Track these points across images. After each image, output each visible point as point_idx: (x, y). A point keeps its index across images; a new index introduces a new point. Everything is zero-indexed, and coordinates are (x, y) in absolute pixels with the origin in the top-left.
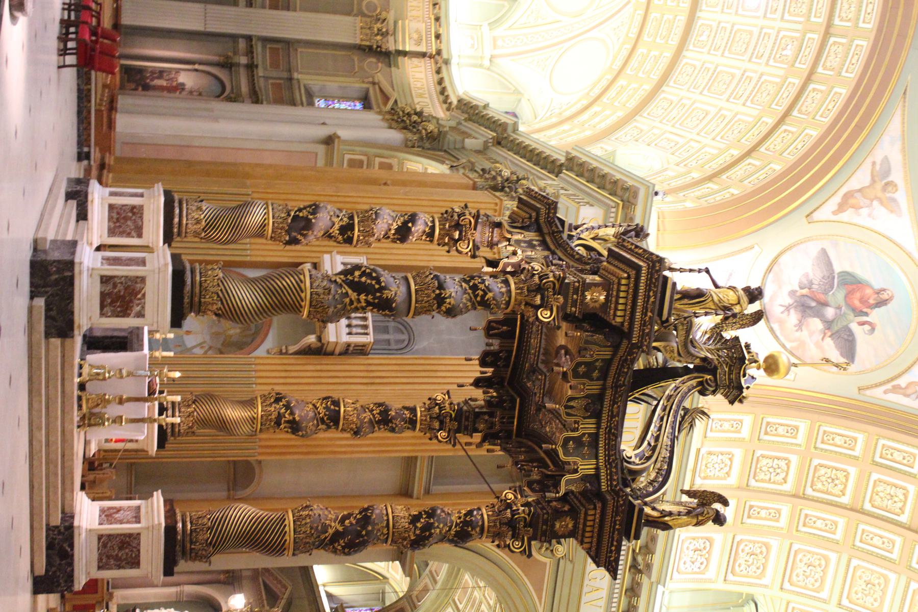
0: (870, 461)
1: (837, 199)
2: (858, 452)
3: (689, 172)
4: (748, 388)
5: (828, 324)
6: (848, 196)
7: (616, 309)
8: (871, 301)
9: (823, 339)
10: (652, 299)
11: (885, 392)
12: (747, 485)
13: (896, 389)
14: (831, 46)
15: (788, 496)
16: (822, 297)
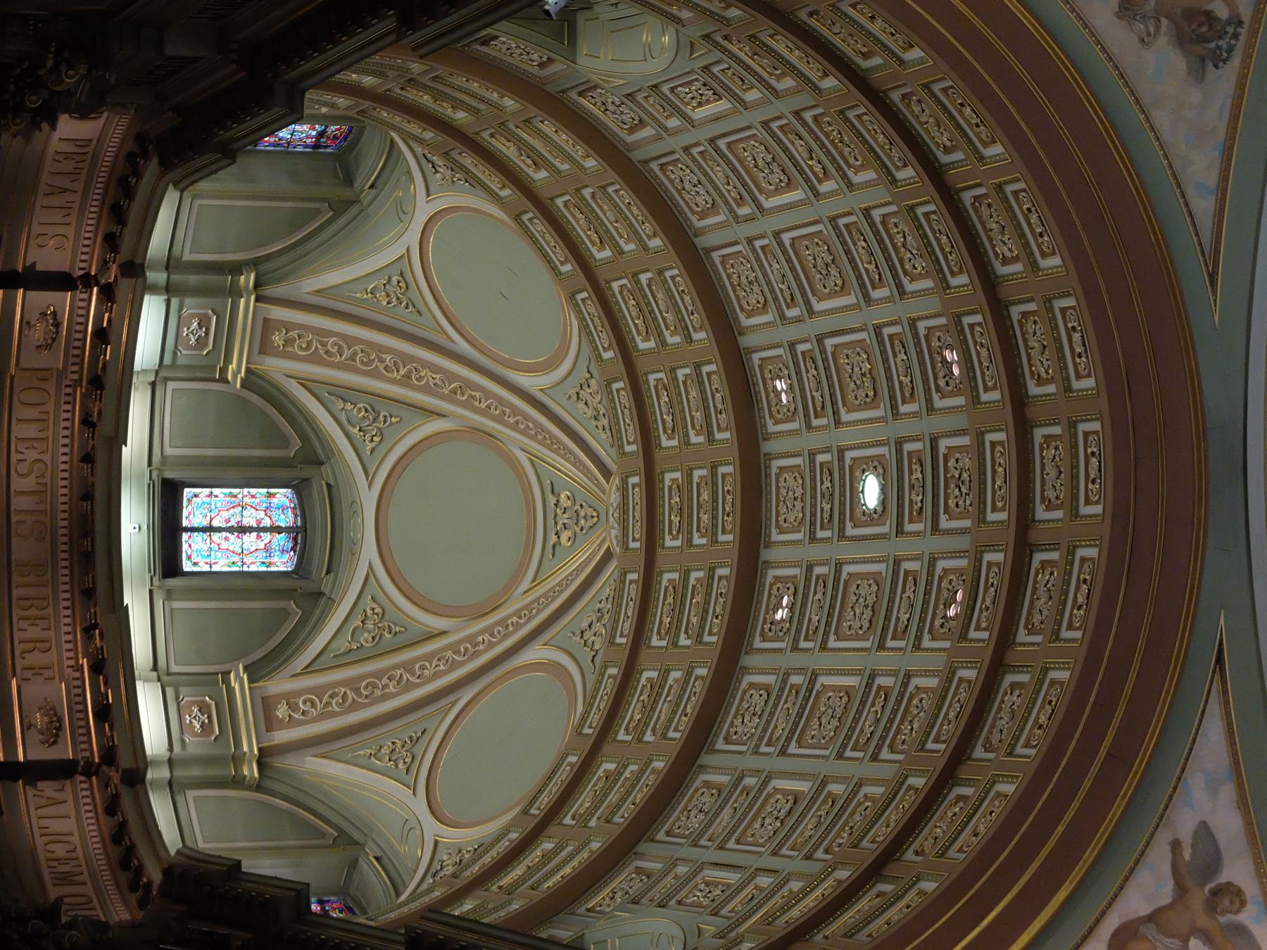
14: (1037, 573)
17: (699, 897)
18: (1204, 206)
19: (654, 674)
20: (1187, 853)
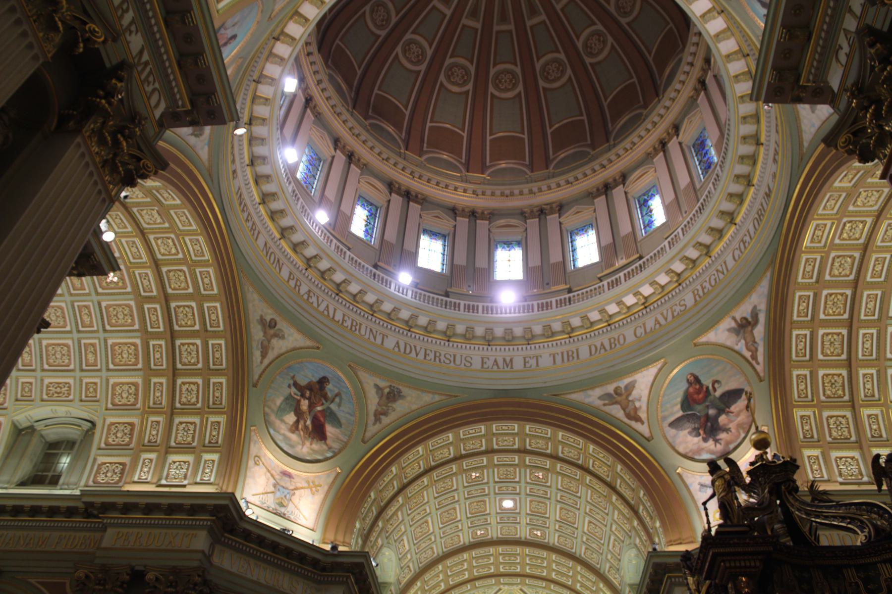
0: (811, 362)
1: (633, 424)
2: (806, 372)
3: (634, 528)
4: (783, 458)
5: (721, 411)
6: (629, 416)
7: (750, 567)
8: (697, 387)
9: (732, 413)
10: (736, 541)
11: (758, 363)
12: (857, 442)
13: (754, 357)
15: (855, 412)
16: (702, 420)
17: (617, 550)
18: (437, 398)
19: (554, 573)
20: (606, 402)
